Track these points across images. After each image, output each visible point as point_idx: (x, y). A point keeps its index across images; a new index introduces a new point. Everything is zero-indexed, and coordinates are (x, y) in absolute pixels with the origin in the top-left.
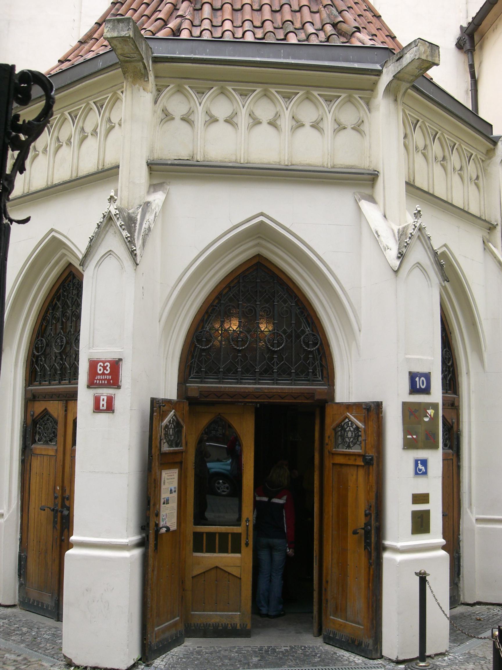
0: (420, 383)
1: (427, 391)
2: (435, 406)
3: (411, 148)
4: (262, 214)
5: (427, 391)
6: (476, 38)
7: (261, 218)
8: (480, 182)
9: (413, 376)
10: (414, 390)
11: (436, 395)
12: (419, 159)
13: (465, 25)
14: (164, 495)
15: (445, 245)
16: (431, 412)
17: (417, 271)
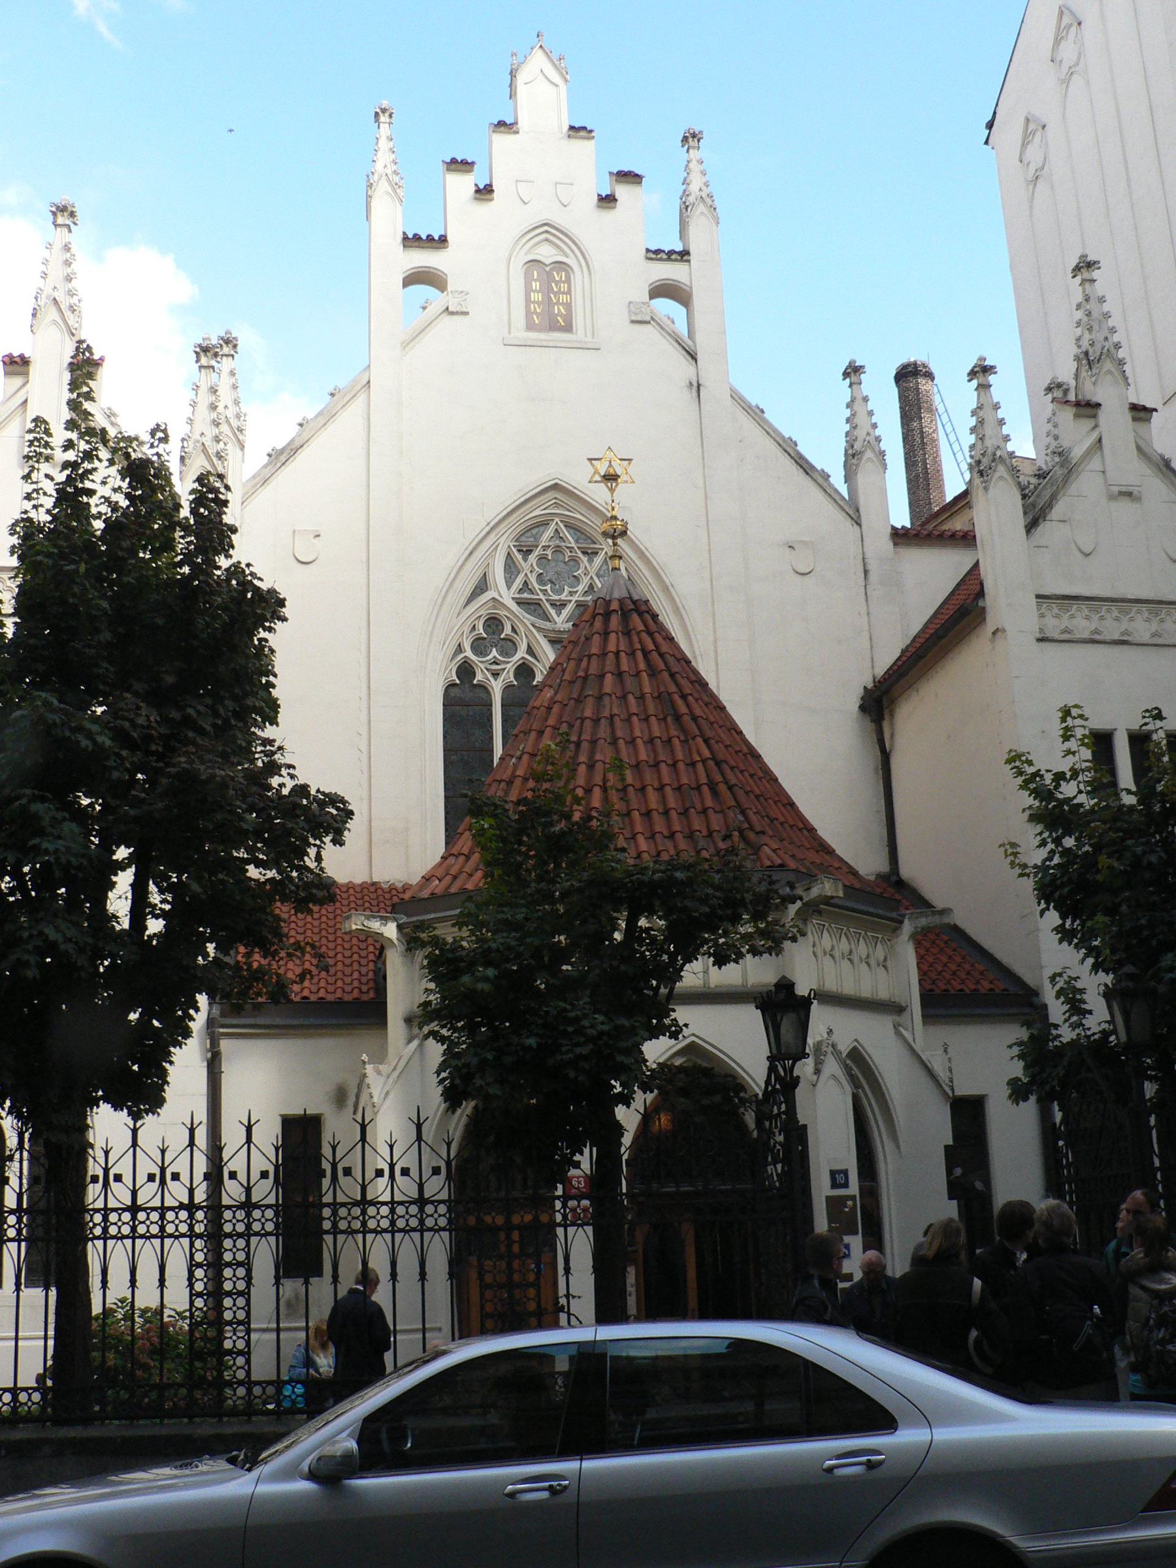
0: (840, 1179)
1: (846, 1185)
2: (853, 1198)
3: (819, 954)
4: (693, 1035)
5: (846, 1185)
6: (885, 702)
7: (693, 1038)
8: (889, 963)
9: (833, 1173)
10: (835, 1185)
11: (854, 1188)
12: (828, 961)
13: (870, 685)
14: (629, 1289)
15: (856, 1040)
16: (850, 1203)
17: (832, 1082)
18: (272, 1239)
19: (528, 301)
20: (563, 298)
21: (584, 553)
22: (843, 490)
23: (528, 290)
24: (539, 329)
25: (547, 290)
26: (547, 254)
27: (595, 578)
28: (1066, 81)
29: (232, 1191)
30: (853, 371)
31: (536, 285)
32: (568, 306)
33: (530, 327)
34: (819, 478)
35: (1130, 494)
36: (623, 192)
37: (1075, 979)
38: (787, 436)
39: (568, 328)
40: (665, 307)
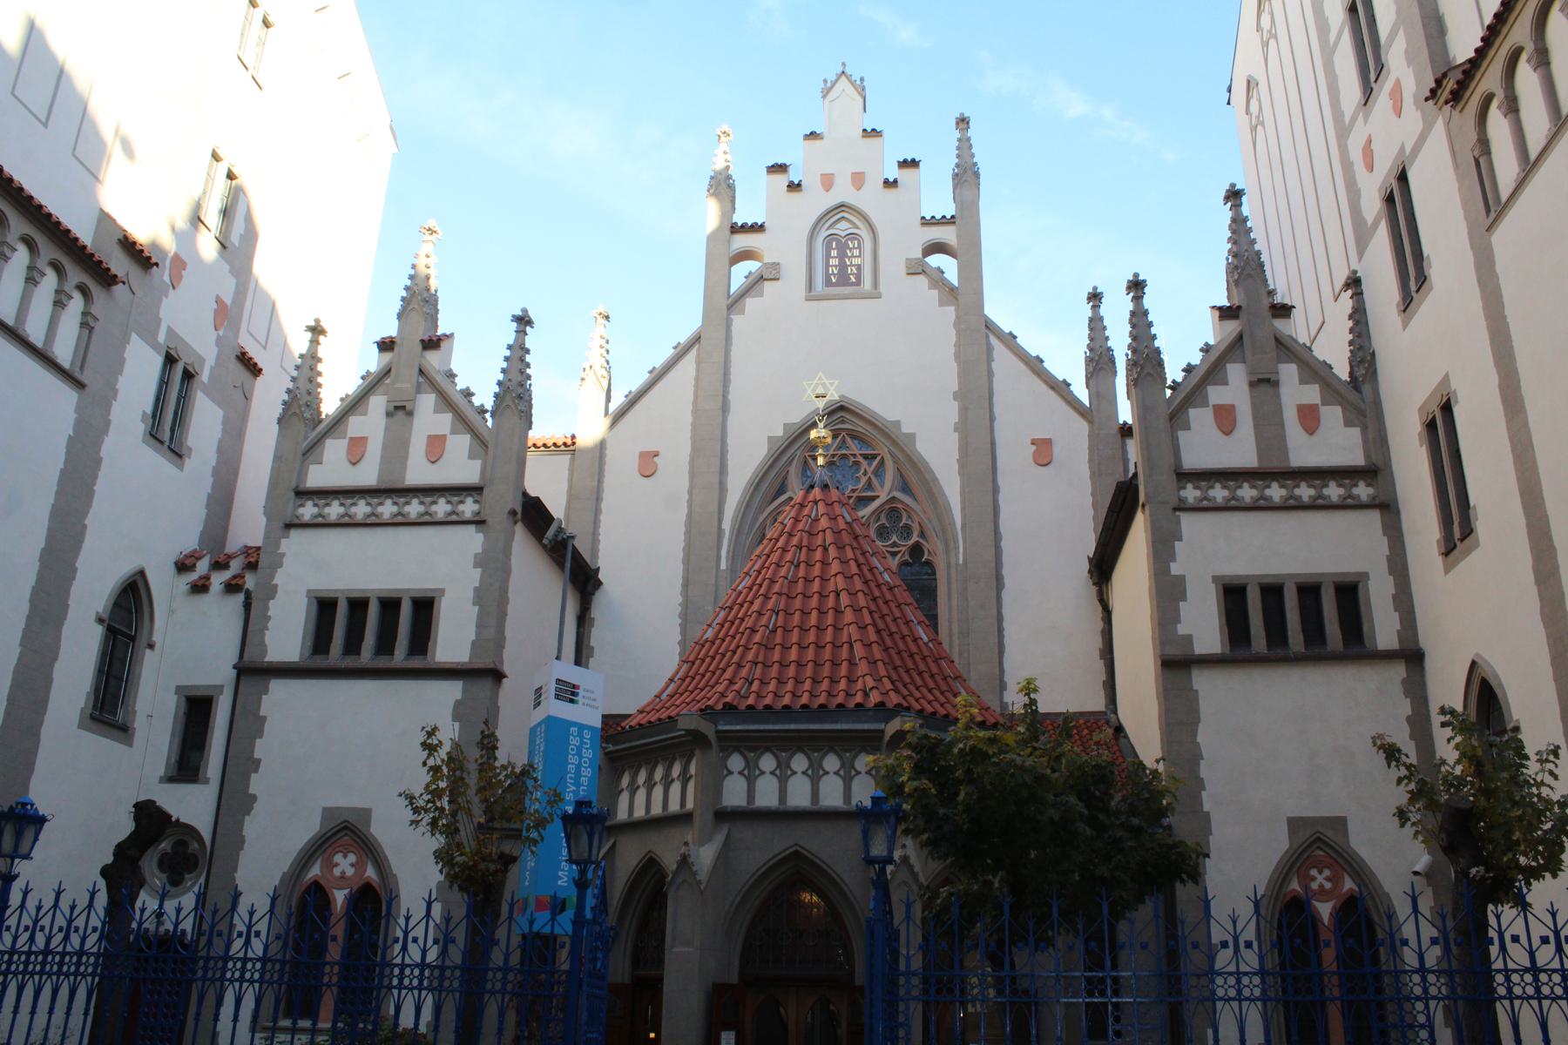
18: (457, 995)
19: (827, 265)
20: (856, 261)
21: (865, 457)
22: (1081, 392)
23: (828, 256)
24: (837, 284)
25: (842, 256)
26: (843, 228)
27: (874, 480)
28: (1265, 45)
29: (497, 957)
30: (1095, 297)
31: (834, 253)
32: (859, 267)
33: (828, 283)
34: (1061, 388)
35: (1268, 381)
36: (905, 176)
37: (411, 798)
38: (1034, 354)
39: (858, 283)
40: (935, 260)
